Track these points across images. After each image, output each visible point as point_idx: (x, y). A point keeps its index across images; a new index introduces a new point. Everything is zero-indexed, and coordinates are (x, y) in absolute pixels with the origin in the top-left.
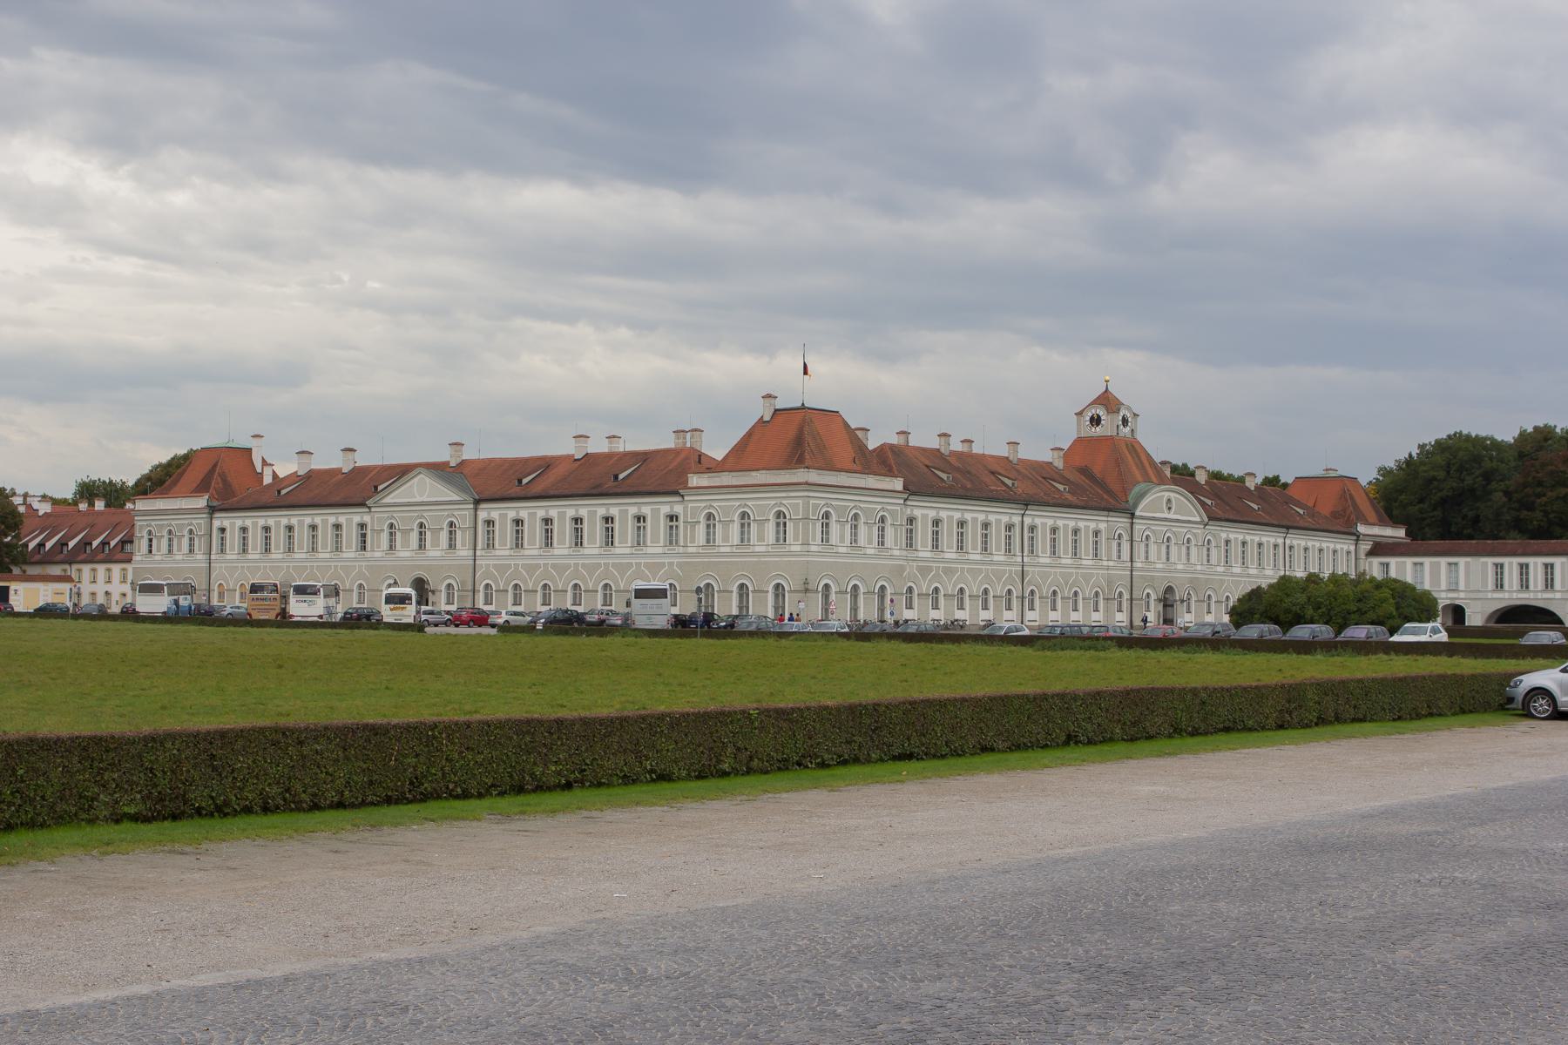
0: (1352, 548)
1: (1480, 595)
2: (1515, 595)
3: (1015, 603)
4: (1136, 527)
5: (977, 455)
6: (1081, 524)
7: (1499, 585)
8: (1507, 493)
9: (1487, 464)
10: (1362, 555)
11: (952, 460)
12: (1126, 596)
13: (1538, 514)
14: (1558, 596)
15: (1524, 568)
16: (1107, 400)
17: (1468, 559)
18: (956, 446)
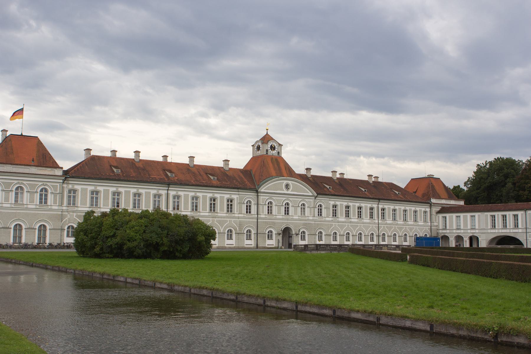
0: (428, 210)
1: (485, 231)
2: (500, 231)
3: (253, 236)
4: (261, 198)
5: (346, 179)
6: (418, 209)
7: (494, 226)
8: (514, 184)
9: (506, 171)
10: (434, 213)
11: (311, 179)
12: (253, 232)
13: (526, 193)
14: (520, 231)
15: (504, 217)
16: (266, 139)
17: (479, 214)
18: (338, 176)
